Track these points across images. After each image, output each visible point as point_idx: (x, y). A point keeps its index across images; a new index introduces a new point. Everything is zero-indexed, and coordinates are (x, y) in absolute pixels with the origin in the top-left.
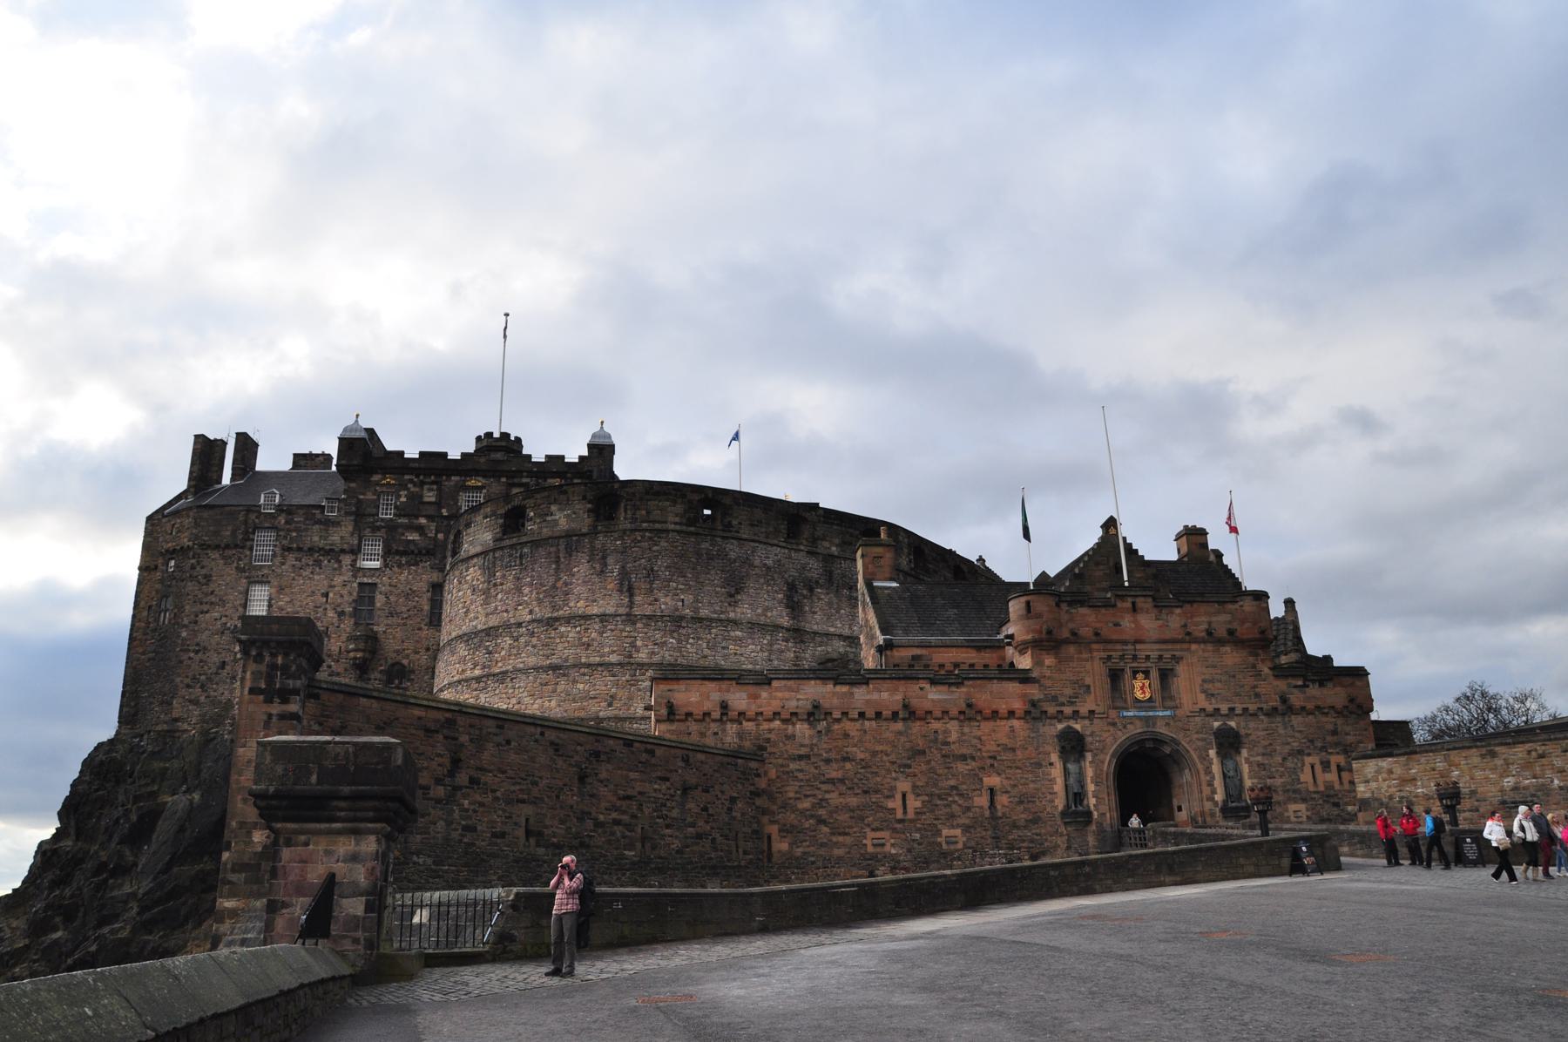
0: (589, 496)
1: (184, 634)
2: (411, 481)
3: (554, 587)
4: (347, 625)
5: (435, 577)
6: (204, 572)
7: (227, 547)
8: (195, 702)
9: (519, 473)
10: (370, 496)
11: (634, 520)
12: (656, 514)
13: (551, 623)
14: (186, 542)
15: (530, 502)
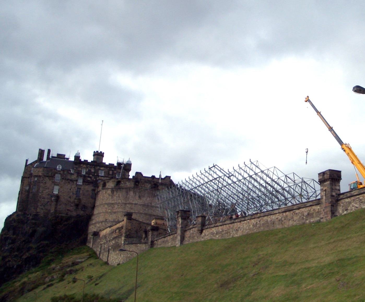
0: (134, 181)
1: (40, 194)
2: (89, 167)
3: (126, 197)
4: (75, 196)
5: (93, 188)
6: (45, 181)
7: (50, 177)
8: (42, 209)
9: (111, 168)
10: (80, 169)
11: (142, 187)
12: (146, 186)
13: (126, 204)
14: (40, 174)
15: (122, 180)
